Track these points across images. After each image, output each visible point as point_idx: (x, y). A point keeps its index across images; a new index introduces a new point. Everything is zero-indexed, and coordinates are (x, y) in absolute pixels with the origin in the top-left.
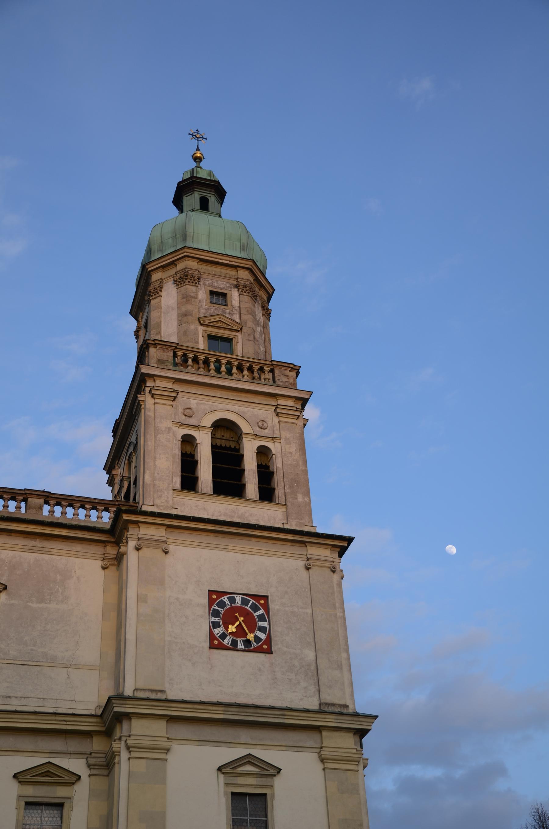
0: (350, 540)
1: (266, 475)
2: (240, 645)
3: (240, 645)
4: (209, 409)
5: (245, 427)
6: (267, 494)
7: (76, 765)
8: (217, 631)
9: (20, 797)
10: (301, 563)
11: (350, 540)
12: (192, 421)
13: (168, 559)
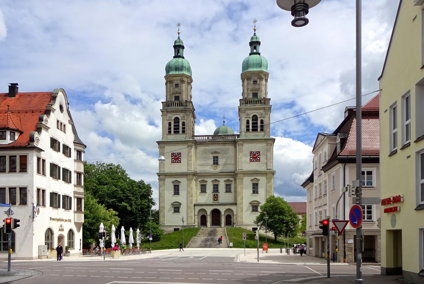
1: (262, 126)
4: (252, 113)
5: (258, 116)
6: (262, 130)
8: (251, 158)
10: (266, 144)
12: (248, 116)
13: (244, 147)
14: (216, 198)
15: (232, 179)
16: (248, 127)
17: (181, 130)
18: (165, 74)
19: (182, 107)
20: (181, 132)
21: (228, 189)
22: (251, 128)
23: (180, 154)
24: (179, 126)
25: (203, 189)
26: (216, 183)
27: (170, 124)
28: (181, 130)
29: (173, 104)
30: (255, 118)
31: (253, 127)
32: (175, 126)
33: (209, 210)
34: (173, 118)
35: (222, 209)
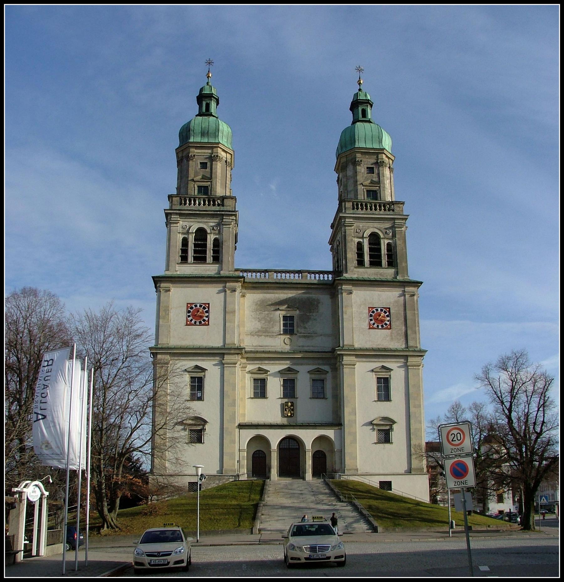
0: (421, 283)
1: (389, 256)
2: (380, 327)
3: (380, 327)
7: (326, 368)
9: (310, 378)
11: (421, 283)
14: (289, 409)
15: (326, 368)
16: (360, 254)
17: (210, 254)
18: (177, 144)
19: (212, 208)
20: (209, 259)
21: (318, 393)
22: (367, 258)
23: (206, 307)
24: (205, 246)
25: (260, 390)
26: (291, 376)
27: (185, 242)
28: (210, 254)
29: (195, 201)
30: (375, 239)
31: (371, 256)
32: (195, 245)
33: (275, 438)
34: (194, 229)
35: (308, 437)
